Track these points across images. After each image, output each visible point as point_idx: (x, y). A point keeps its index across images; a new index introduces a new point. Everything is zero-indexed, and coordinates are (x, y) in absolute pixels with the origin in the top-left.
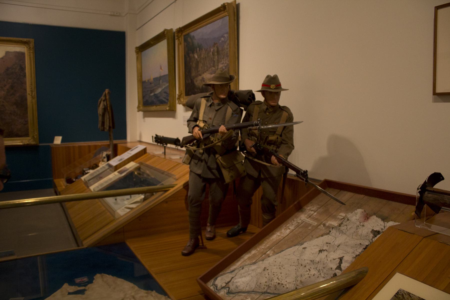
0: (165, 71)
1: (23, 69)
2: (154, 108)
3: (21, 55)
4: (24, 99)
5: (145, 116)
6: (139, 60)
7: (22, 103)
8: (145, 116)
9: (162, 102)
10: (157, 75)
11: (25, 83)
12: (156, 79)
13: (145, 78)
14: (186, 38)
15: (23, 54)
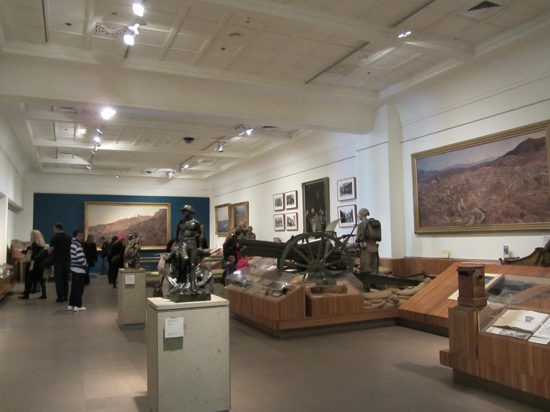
0: (227, 219)
1: (166, 216)
2: (223, 233)
3: (165, 211)
4: (166, 229)
5: (219, 237)
6: (216, 212)
7: (165, 231)
8: (219, 237)
9: (227, 231)
10: (224, 220)
11: (166, 222)
12: (224, 221)
13: (219, 220)
14: (235, 208)
15: (166, 210)
